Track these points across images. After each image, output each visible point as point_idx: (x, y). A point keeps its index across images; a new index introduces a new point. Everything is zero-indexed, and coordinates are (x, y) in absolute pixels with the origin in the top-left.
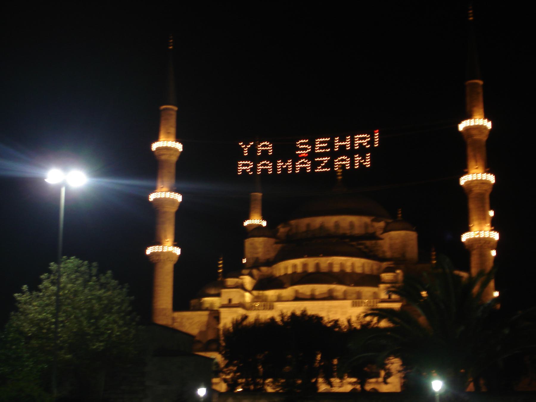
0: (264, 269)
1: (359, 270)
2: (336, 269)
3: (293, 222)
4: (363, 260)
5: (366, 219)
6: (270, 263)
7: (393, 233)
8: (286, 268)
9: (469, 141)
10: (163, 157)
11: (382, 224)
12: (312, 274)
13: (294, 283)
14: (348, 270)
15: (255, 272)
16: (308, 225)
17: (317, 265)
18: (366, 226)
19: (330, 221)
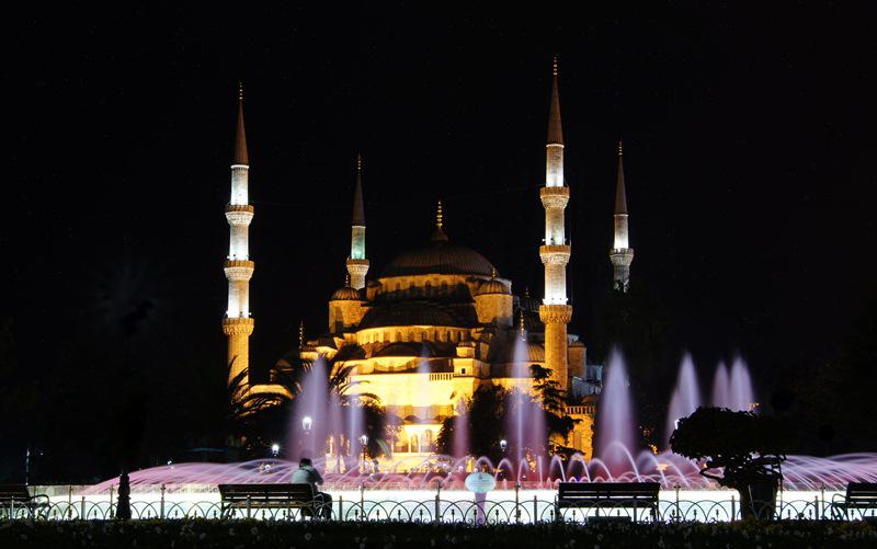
0: (347, 335)
1: (441, 339)
2: (417, 339)
3: (382, 281)
4: (448, 328)
5: (462, 279)
6: (354, 329)
7: (484, 296)
8: (368, 337)
9: (547, 209)
10: (234, 222)
11: (476, 284)
12: (393, 344)
13: (375, 354)
14: (433, 340)
15: (337, 340)
16: (398, 285)
17: (399, 335)
18: (462, 287)
19: (422, 280)
